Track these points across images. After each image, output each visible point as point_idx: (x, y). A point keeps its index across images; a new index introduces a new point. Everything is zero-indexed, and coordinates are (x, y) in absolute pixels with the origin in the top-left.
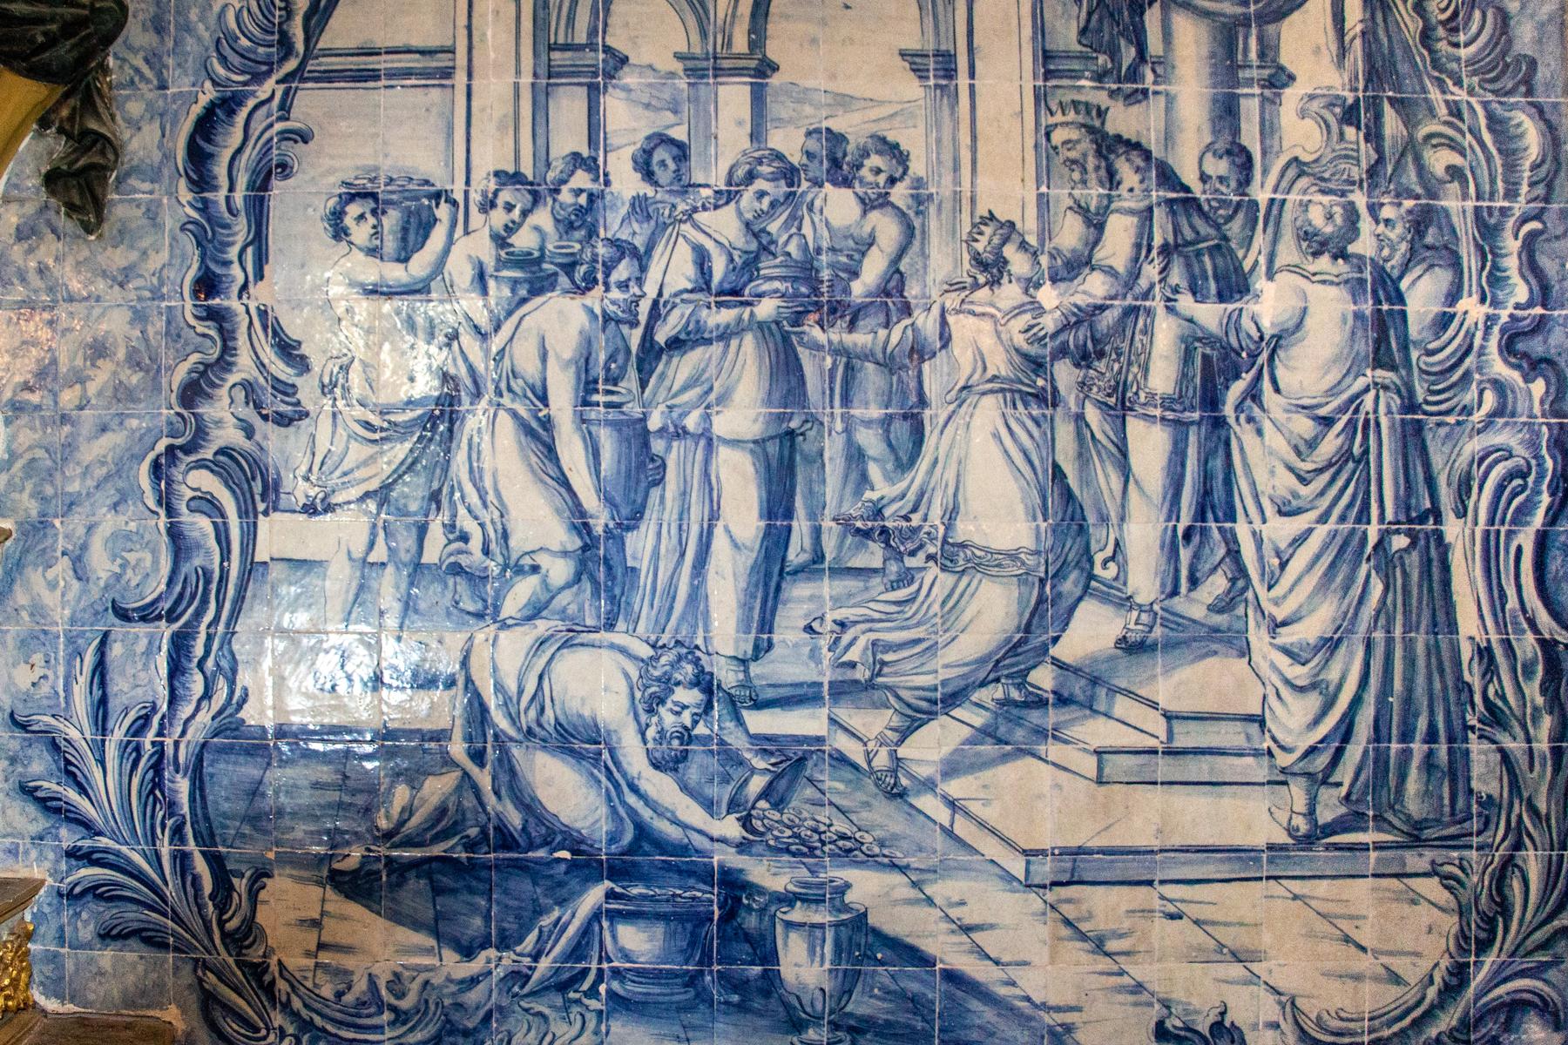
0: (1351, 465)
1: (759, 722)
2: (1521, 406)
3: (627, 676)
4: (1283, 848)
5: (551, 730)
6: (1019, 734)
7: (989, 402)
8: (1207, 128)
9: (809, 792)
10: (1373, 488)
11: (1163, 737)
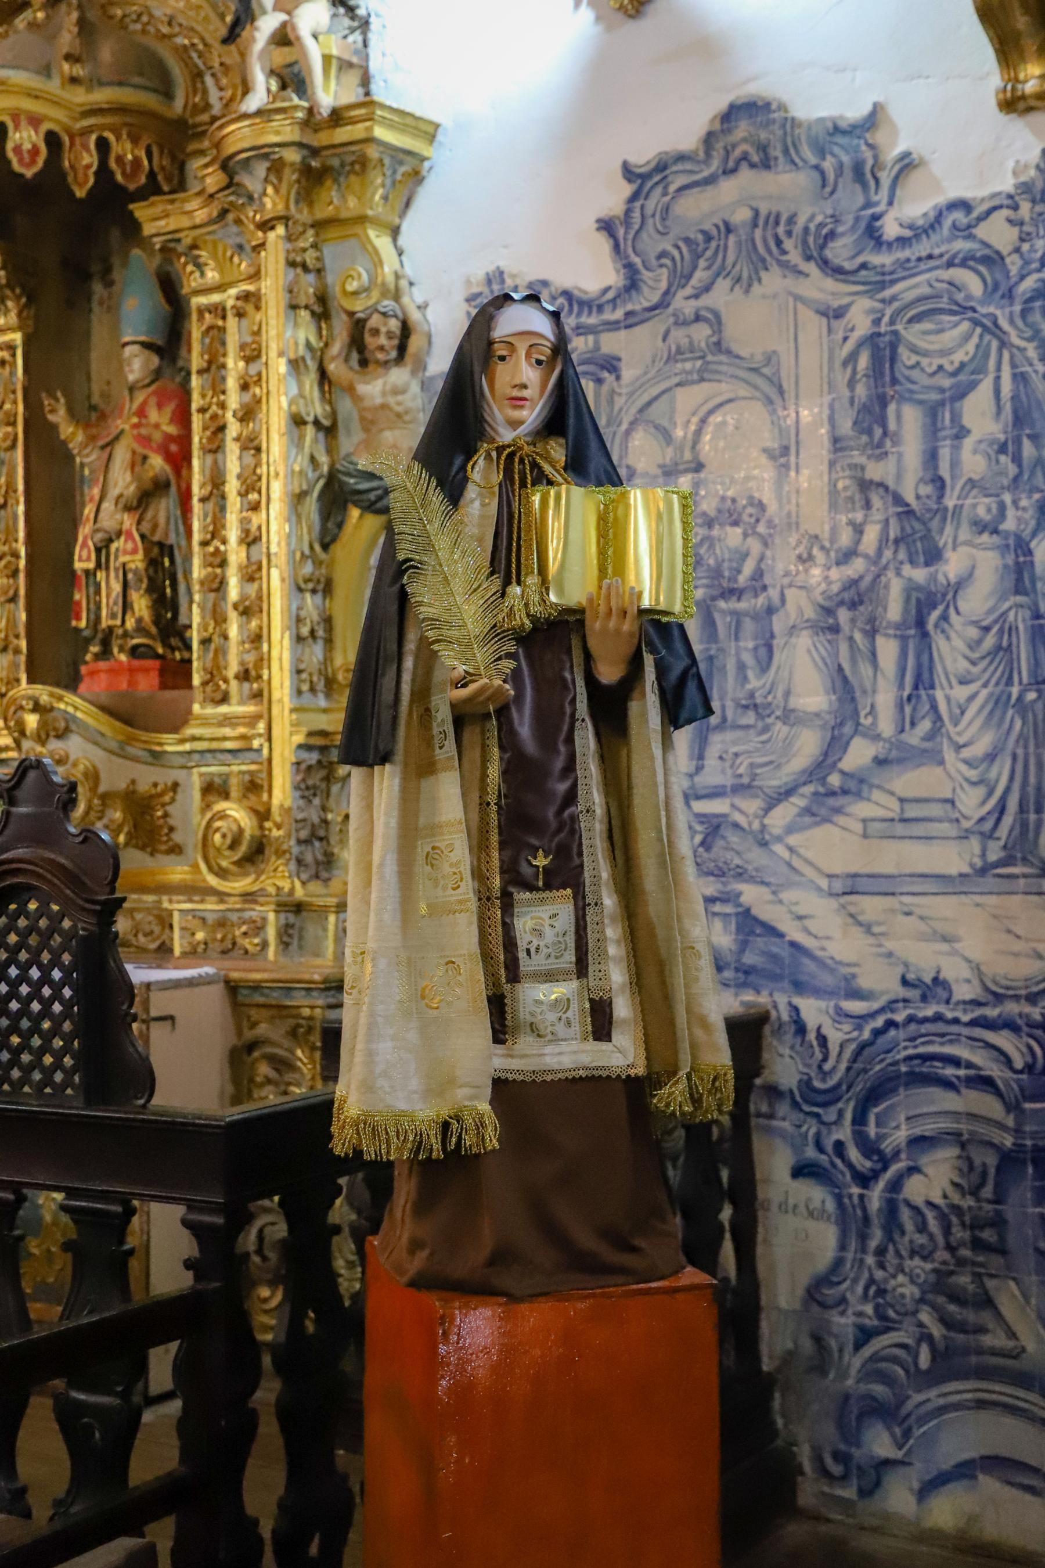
6: (823, 811)
7: (805, 633)
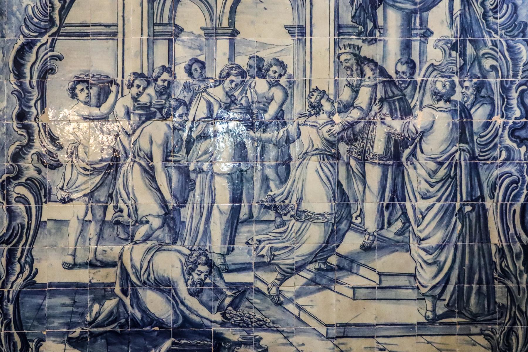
0: (450, 180)
1: (229, 278)
2: (517, 157)
3: (181, 261)
4: (423, 324)
5: (153, 282)
6: (324, 281)
7: (314, 158)
8: (399, 53)
9: (247, 303)
10: (458, 188)
11: (378, 282)
